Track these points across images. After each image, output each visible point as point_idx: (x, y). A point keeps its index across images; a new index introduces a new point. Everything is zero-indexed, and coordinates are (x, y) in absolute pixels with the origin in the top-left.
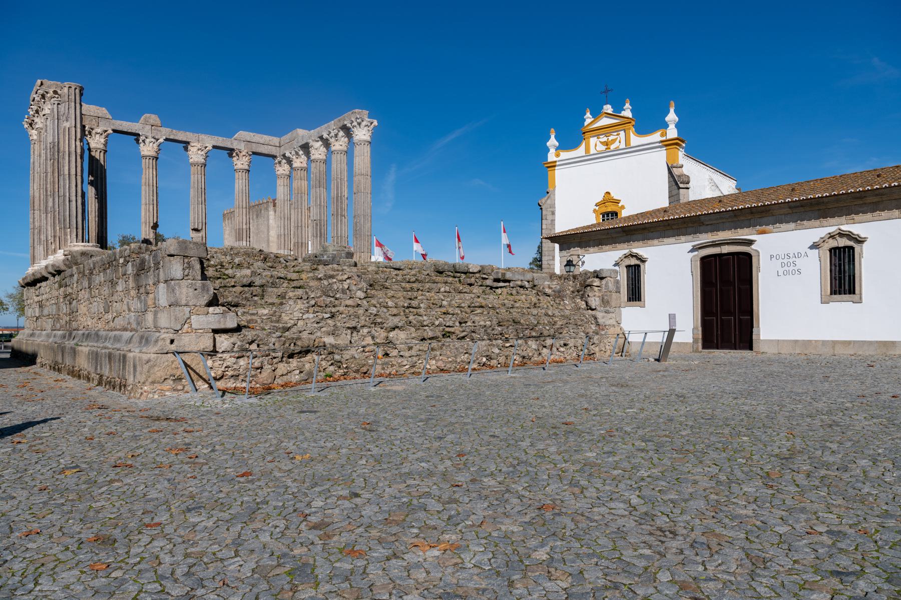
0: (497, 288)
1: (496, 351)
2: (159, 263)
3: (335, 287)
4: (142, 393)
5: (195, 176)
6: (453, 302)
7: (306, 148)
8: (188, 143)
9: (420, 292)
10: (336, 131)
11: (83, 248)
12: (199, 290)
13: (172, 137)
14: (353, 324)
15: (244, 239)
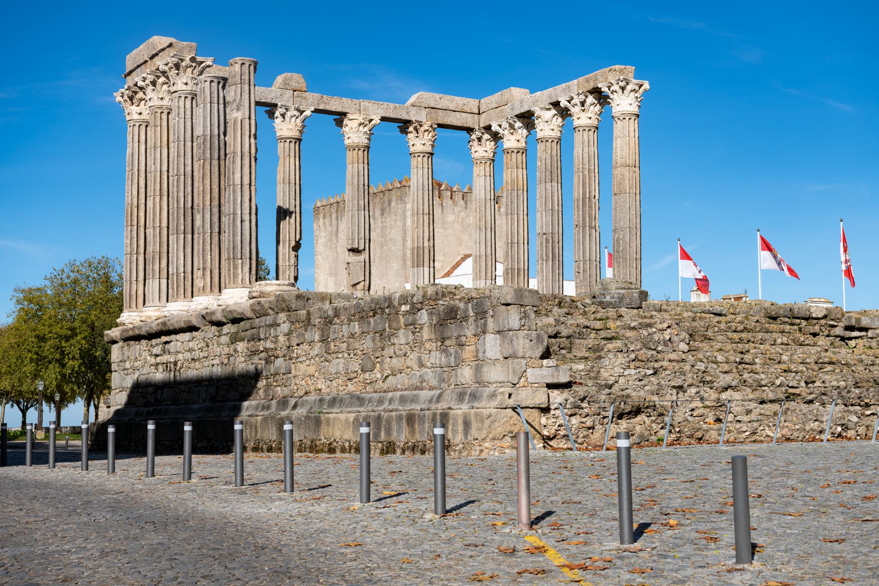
0: (850, 339)
1: (855, 419)
2: (486, 312)
3: (656, 337)
5: (353, 167)
6: (795, 357)
7: (527, 118)
10: (582, 97)
12: (534, 341)
14: (678, 382)
15: (426, 264)
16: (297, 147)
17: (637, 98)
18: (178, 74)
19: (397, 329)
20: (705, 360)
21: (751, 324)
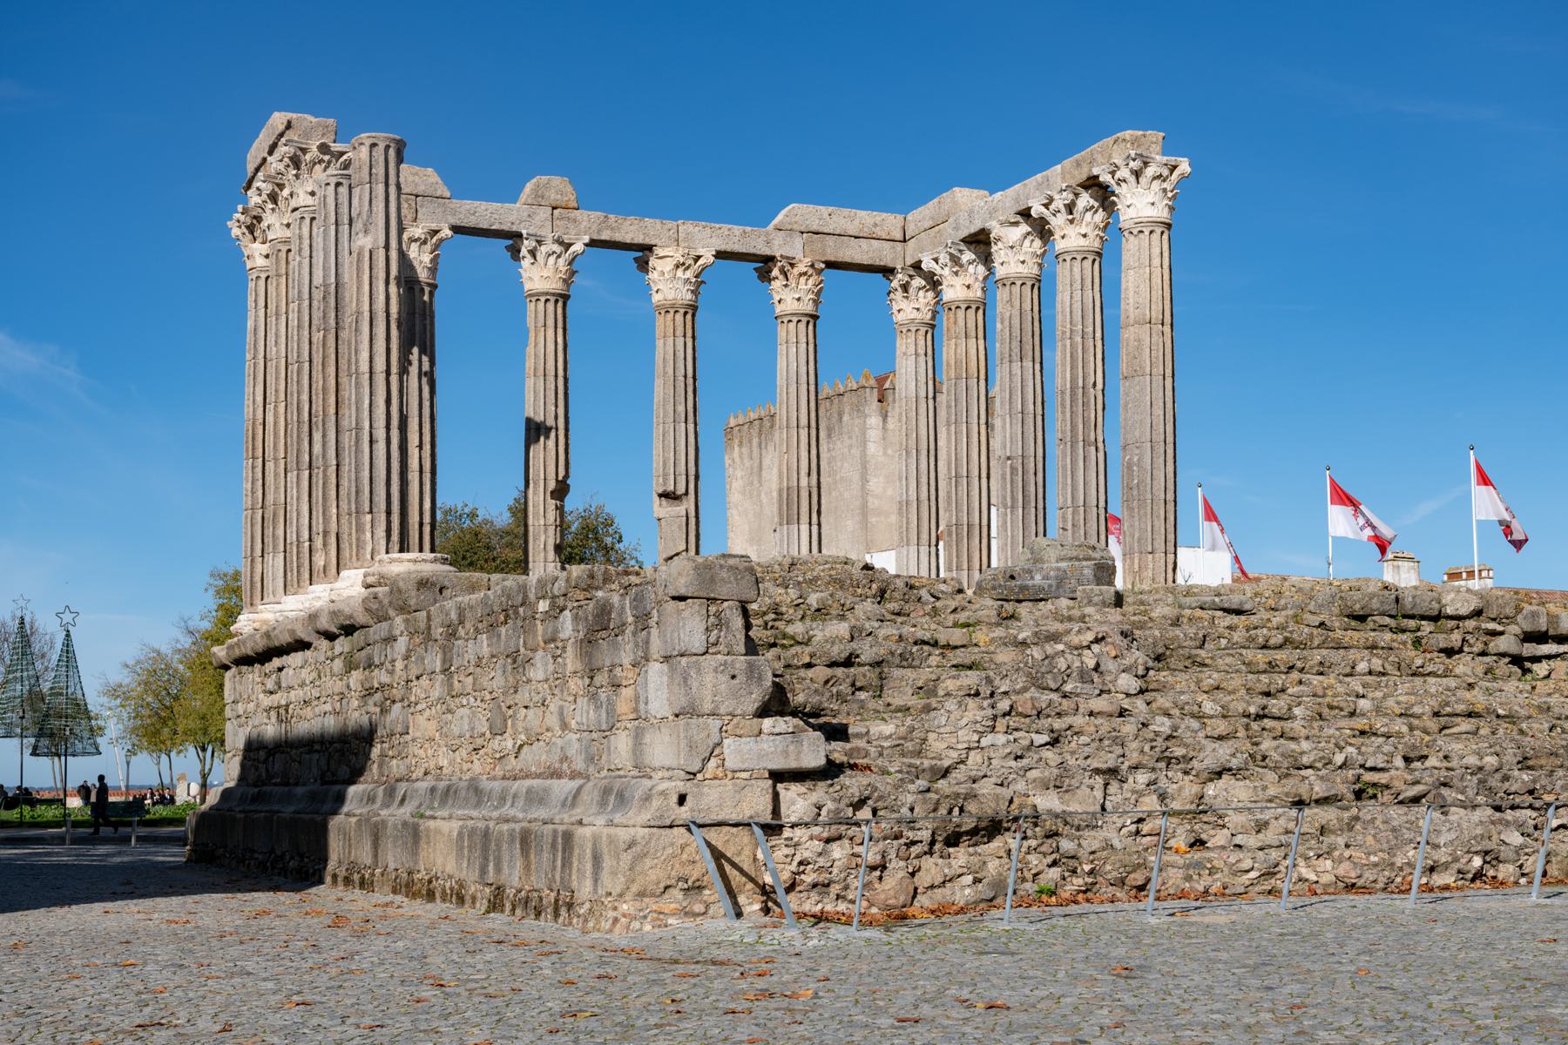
0: (1537, 659)
1: (1515, 838)
2: (648, 615)
3: (1062, 664)
4: (616, 920)
5: (667, 345)
6: (1390, 702)
7: (980, 242)
8: (649, 248)
9: (1295, 675)
11: (412, 567)
12: (741, 678)
13: (605, 236)
14: (1107, 760)
16: (560, 311)
17: (1165, 190)
18: (297, 176)
19: (534, 650)
20: (1176, 712)
21: (1300, 633)
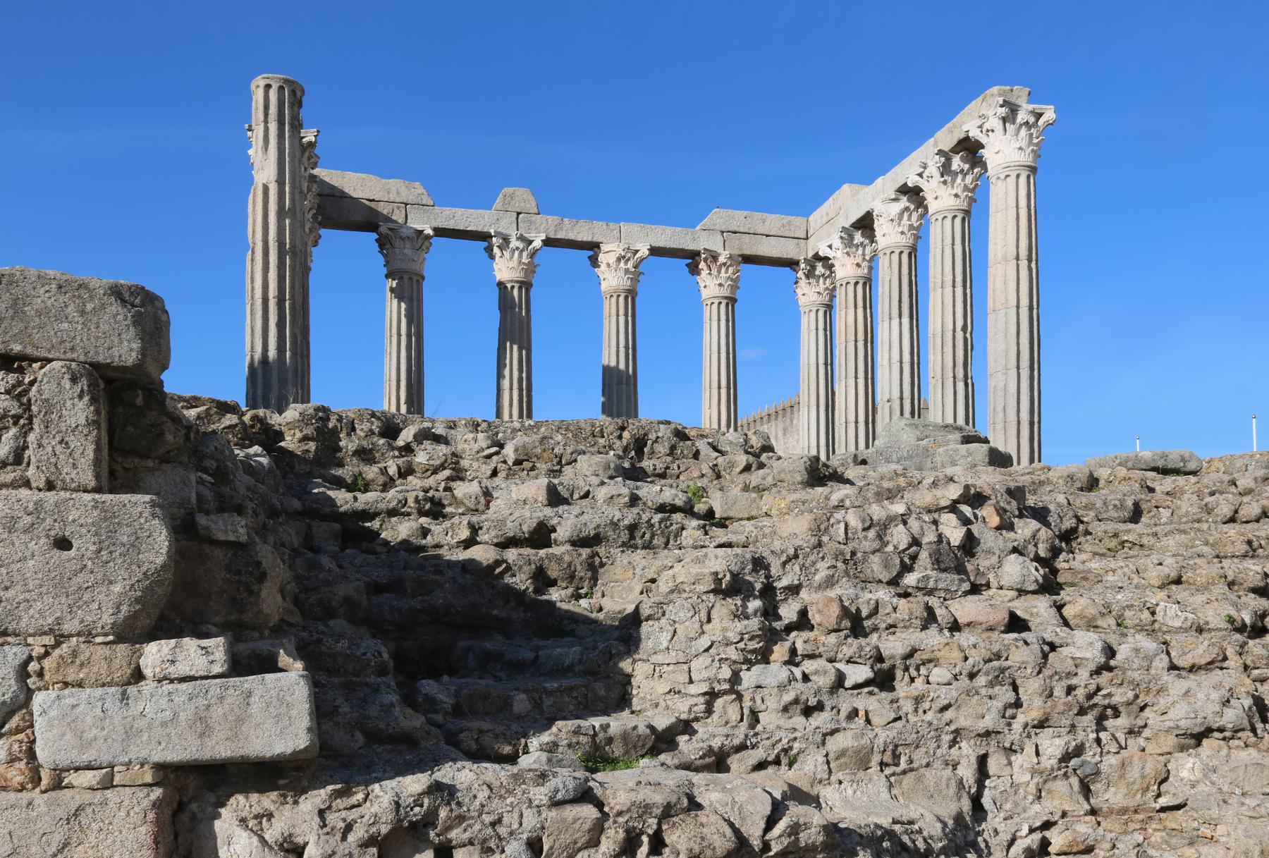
3: (899, 536)
8: (594, 247)
